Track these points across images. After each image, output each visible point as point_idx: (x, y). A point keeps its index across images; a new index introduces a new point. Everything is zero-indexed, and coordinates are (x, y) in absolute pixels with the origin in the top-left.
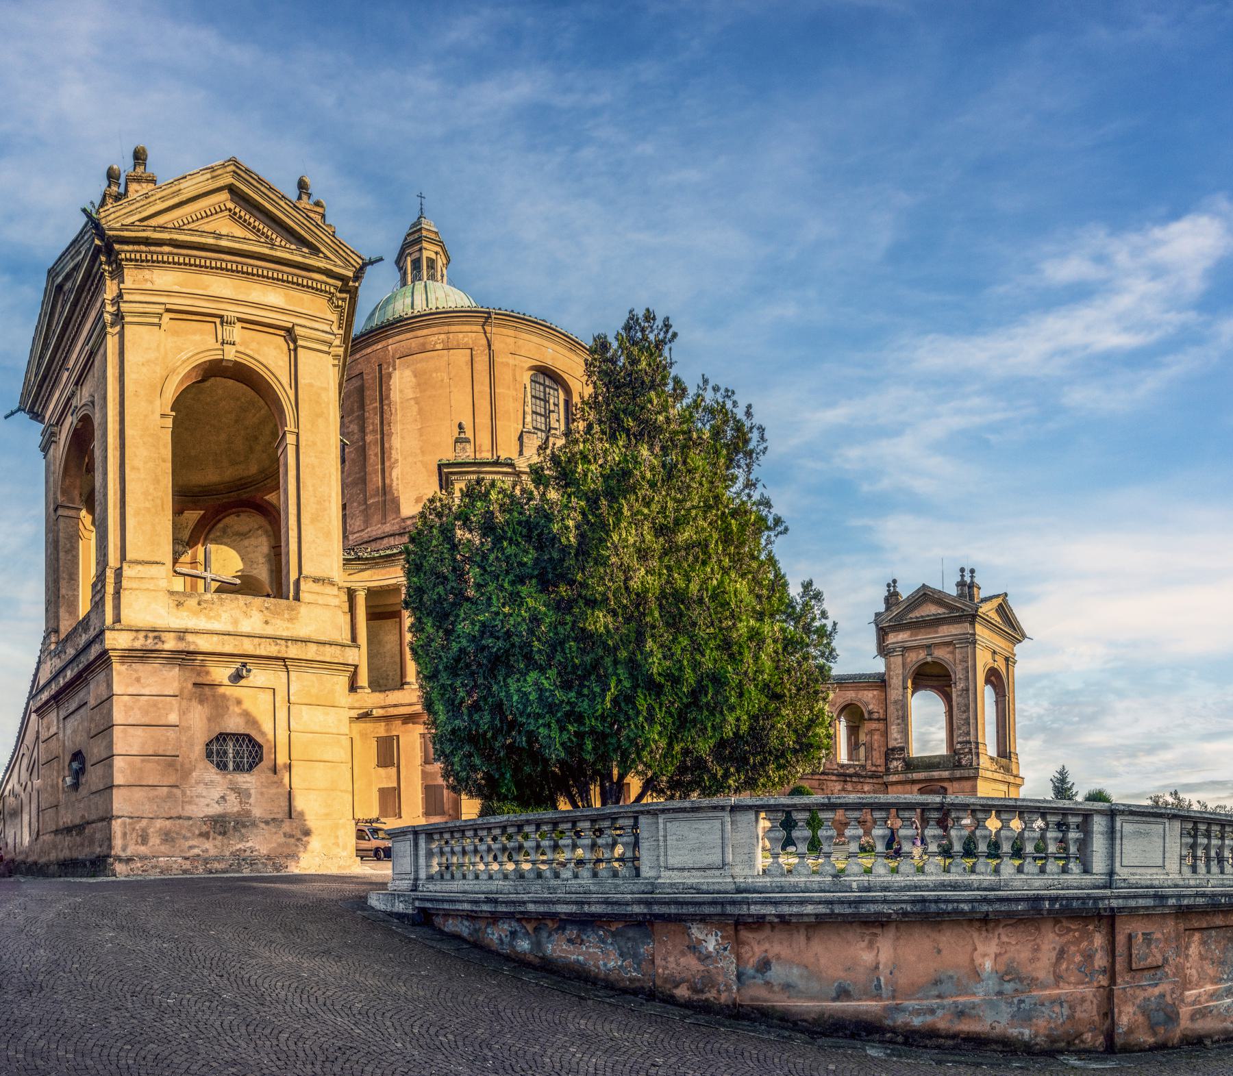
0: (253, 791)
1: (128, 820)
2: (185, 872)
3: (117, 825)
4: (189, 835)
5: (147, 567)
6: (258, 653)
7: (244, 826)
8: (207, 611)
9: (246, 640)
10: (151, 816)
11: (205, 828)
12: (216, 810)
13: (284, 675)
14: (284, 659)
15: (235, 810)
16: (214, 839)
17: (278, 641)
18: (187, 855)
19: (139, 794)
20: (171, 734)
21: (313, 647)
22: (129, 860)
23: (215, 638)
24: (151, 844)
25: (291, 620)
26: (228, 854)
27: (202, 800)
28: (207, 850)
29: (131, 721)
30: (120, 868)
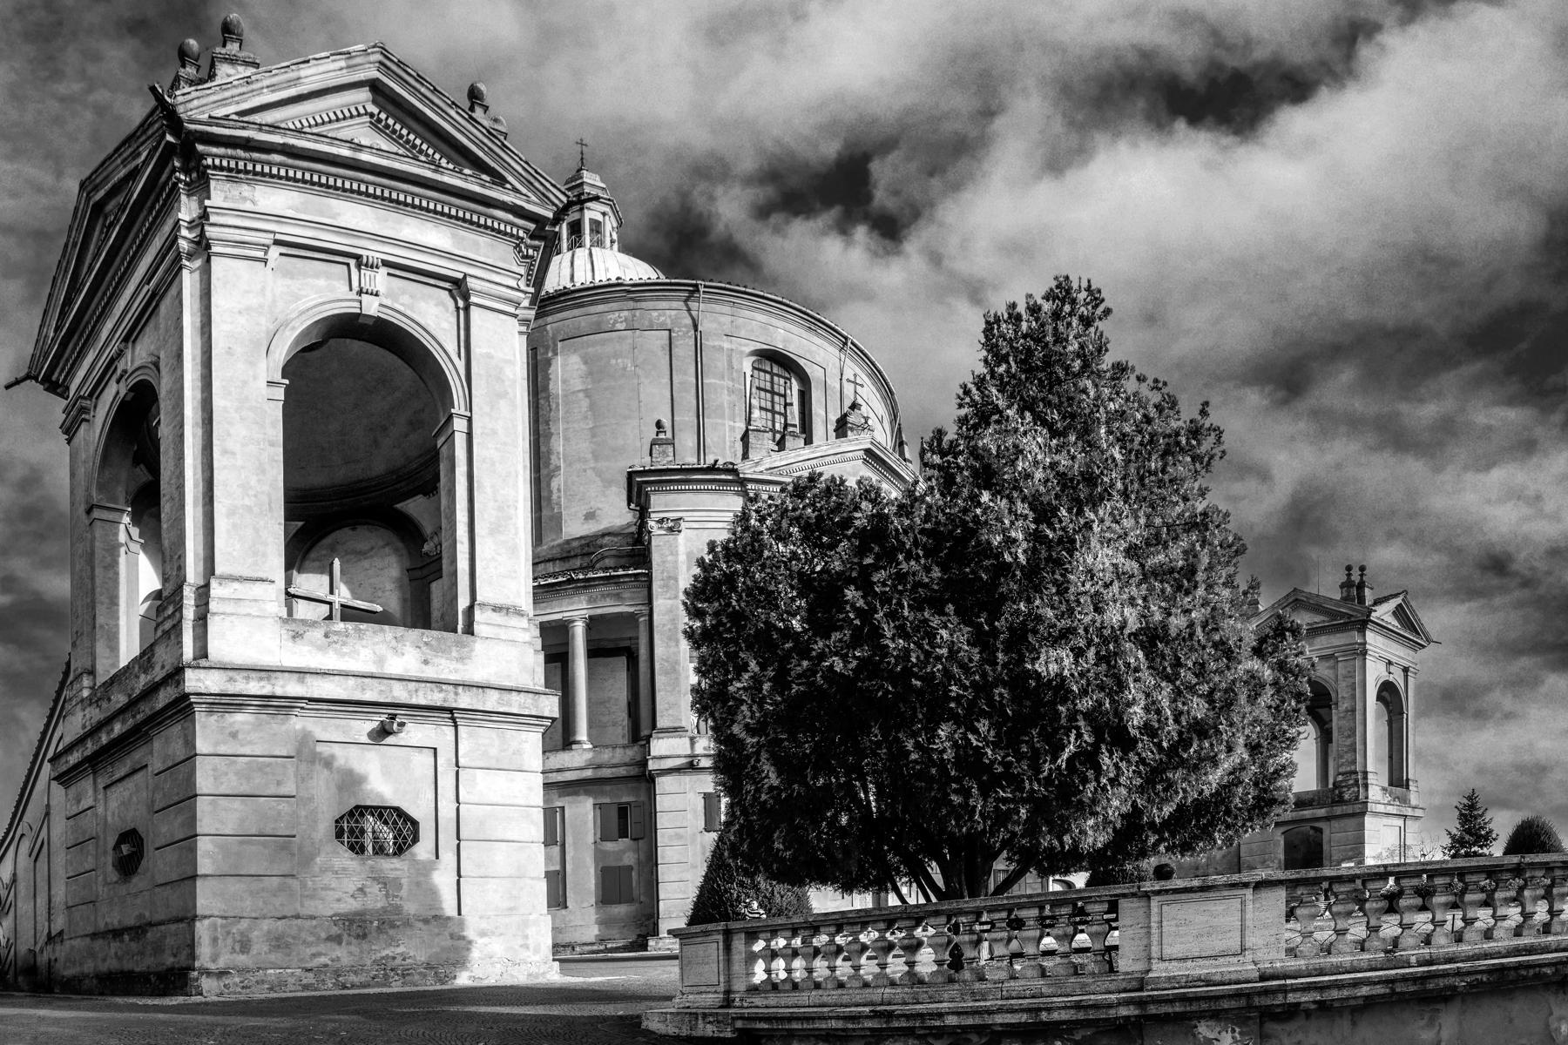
0: (404, 881)
1: (220, 921)
2: (306, 987)
3: (202, 928)
4: (311, 939)
6: (414, 701)
7: (393, 926)
8: (338, 646)
9: (397, 686)
10: (254, 915)
11: (335, 930)
12: (350, 905)
13: (450, 731)
14: (451, 710)
15: (379, 905)
16: (349, 943)
17: (444, 687)
18: (309, 966)
19: (235, 886)
20: (283, 806)
21: (494, 695)
22: (222, 974)
23: (351, 681)
24: (254, 951)
25: (461, 659)
26: (369, 962)
27: (331, 893)
28: (338, 959)
29: (222, 790)
30: (207, 984)
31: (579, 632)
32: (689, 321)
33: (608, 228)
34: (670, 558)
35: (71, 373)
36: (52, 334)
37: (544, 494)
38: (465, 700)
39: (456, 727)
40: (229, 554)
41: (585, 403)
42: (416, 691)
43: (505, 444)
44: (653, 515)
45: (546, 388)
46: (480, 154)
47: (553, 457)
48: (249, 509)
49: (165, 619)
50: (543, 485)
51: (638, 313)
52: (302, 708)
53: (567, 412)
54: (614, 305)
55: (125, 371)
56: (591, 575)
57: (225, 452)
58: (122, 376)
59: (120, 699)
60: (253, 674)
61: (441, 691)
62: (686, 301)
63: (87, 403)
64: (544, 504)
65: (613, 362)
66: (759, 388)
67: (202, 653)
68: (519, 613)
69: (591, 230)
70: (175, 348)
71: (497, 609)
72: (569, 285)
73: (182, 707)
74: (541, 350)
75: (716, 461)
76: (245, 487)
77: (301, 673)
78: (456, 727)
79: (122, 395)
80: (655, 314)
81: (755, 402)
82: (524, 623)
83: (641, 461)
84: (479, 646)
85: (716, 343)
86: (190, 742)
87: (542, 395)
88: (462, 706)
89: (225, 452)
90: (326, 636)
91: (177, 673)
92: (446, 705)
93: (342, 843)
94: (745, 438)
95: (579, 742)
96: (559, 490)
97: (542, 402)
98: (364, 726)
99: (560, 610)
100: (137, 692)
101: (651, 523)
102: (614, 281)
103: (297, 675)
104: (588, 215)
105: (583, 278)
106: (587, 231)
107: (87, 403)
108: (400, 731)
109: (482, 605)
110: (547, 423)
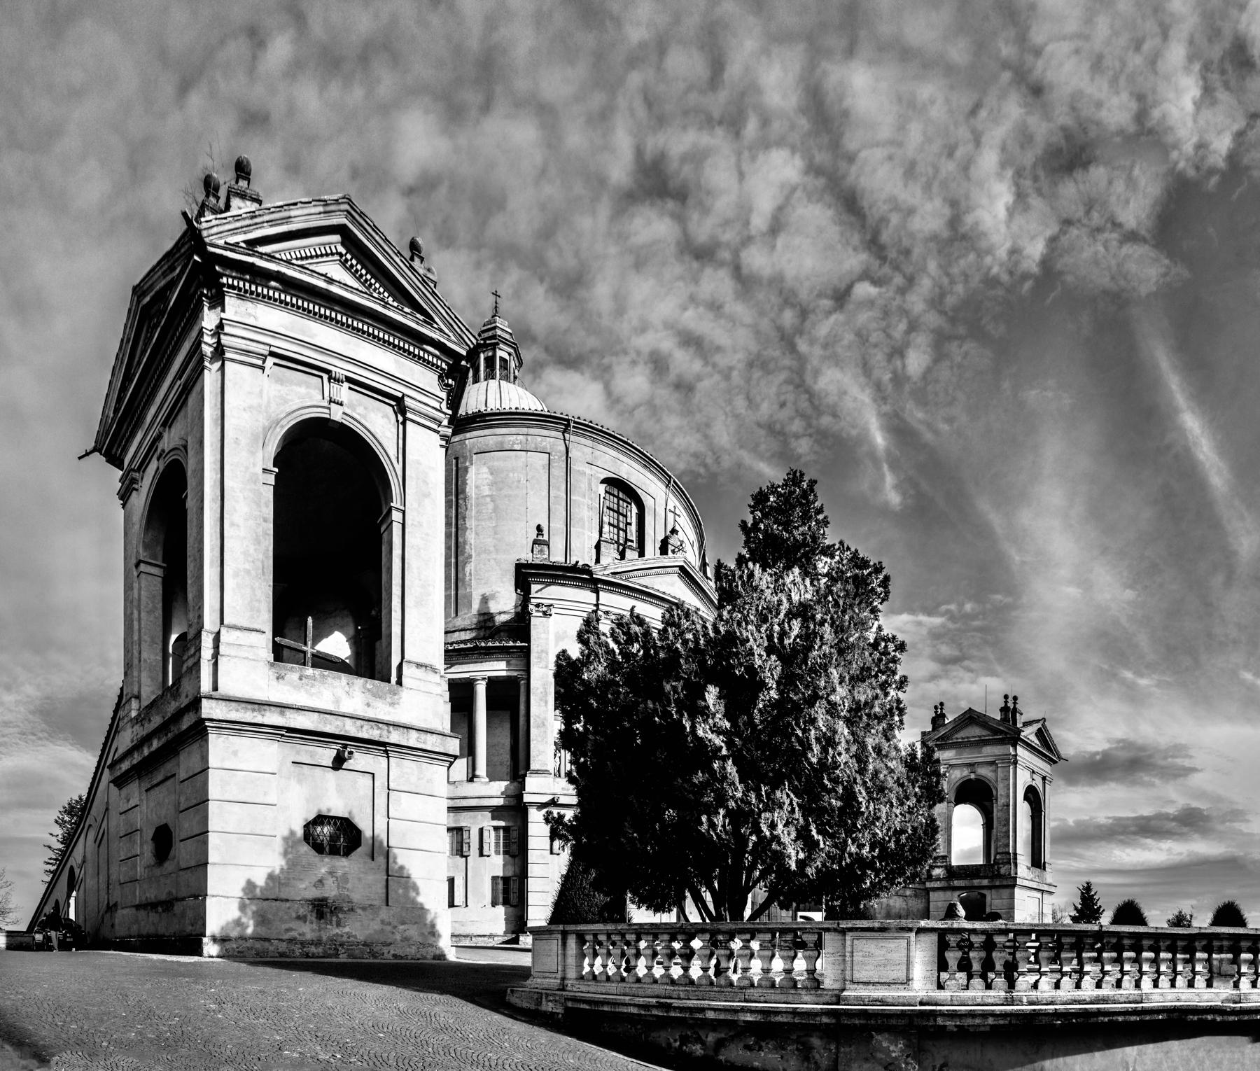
5: (247, 634)
6: (360, 735)
9: (348, 722)
14: (384, 744)
17: (380, 725)
21: (414, 734)
25: (392, 704)
31: (481, 690)
32: (564, 449)
33: (513, 365)
34: (543, 636)
35: (125, 450)
36: (112, 415)
37: (460, 576)
38: (395, 737)
39: (388, 757)
40: (235, 608)
41: (491, 506)
42: (362, 727)
43: (427, 535)
44: (532, 600)
45: (464, 491)
46: (417, 297)
47: (467, 547)
48: (248, 572)
49: (189, 658)
50: (460, 568)
51: (529, 437)
52: (283, 735)
53: (477, 512)
54: (513, 430)
55: (163, 451)
56: (490, 644)
57: (232, 524)
58: (161, 455)
59: (157, 720)
60: (250, 706)
61: (379, 728)
62: (563, 433)
63: (136, 475)
64: (460, 584)
65: (511, 475)
66: (608, 508)
67: (215, 688)
68: (434, 670)
69: (501, 366)
70: (198, 435)
71: (419, 665)
72: (483, 409)
73: (199, 731)
74: (461, 460)
75: (577, 562)
76: (246, 554)
77: (282, 707)
78: (388, 757)
79: (161, 470)
80: (539, 439)
81: (606, 519)
82: (436, 678)
83: (526, 556)
84: (405, 694)
85: (581, 469)
86: (205, 758)
87: (461, 496)
88: (392, 742)
89: (232, 524)
90: (301, 679)
91: (196, 703)
92: (381, 740)
93: (308, 843)
94: (598, 547)
95: (478, 777)
96: (470, 574)
97: (460, 501)
98: (327, 754)
99: (463, 671)
100: (169, 715)
101: (531, 607)
102: (513, 410)
103: (279, 709)
104: (499, 353)
105: (493, 405)
106: (498, 367)
107: (136, 475)
108: (350, 758)
109: (409, 662)
110: (464, 519)
